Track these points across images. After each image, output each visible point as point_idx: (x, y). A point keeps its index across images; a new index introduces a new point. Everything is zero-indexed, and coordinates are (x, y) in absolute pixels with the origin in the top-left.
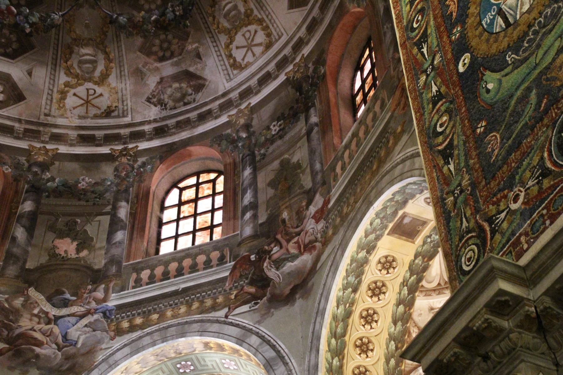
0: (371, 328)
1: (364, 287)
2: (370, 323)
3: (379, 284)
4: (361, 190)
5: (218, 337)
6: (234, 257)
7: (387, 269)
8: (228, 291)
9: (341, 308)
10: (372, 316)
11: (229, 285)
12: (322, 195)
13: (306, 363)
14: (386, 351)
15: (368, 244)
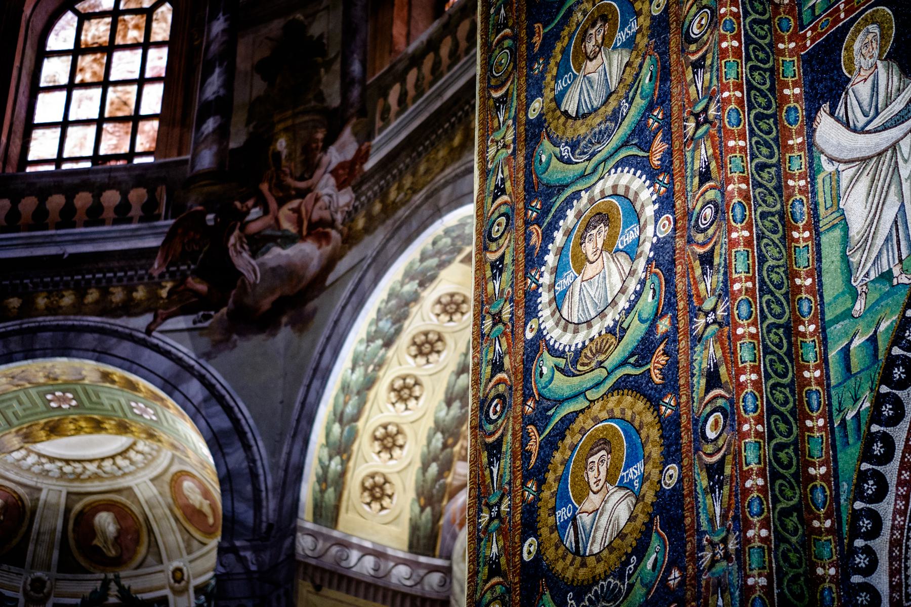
0: (407, 409)
1: (404, 339)
2: (405, 400)
3: (432, 337)
4: (427, 171)
5: (130, 370)
6: (175, 209)
7: (451, 314)
8: (156, 280)
9: (359, 371)
10: (410, 388)
11: (159, 266)
12: (355, 134)
13: (284, 455)
14: (425, 449)
15: (423, 272)
